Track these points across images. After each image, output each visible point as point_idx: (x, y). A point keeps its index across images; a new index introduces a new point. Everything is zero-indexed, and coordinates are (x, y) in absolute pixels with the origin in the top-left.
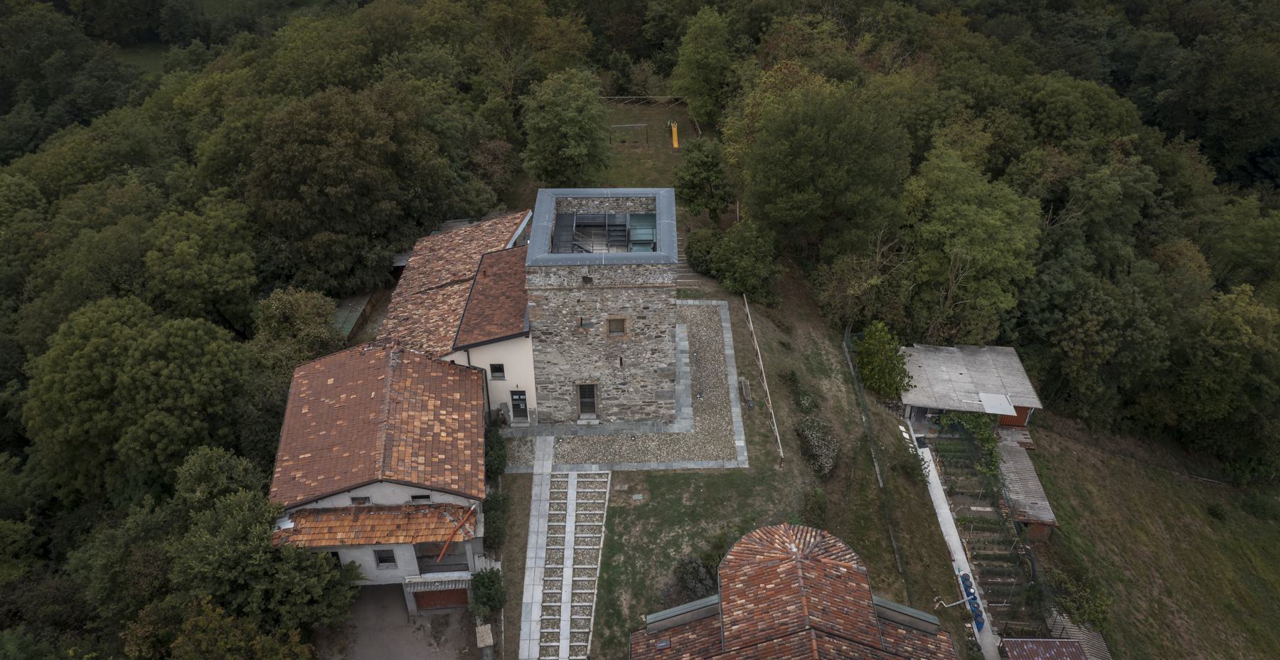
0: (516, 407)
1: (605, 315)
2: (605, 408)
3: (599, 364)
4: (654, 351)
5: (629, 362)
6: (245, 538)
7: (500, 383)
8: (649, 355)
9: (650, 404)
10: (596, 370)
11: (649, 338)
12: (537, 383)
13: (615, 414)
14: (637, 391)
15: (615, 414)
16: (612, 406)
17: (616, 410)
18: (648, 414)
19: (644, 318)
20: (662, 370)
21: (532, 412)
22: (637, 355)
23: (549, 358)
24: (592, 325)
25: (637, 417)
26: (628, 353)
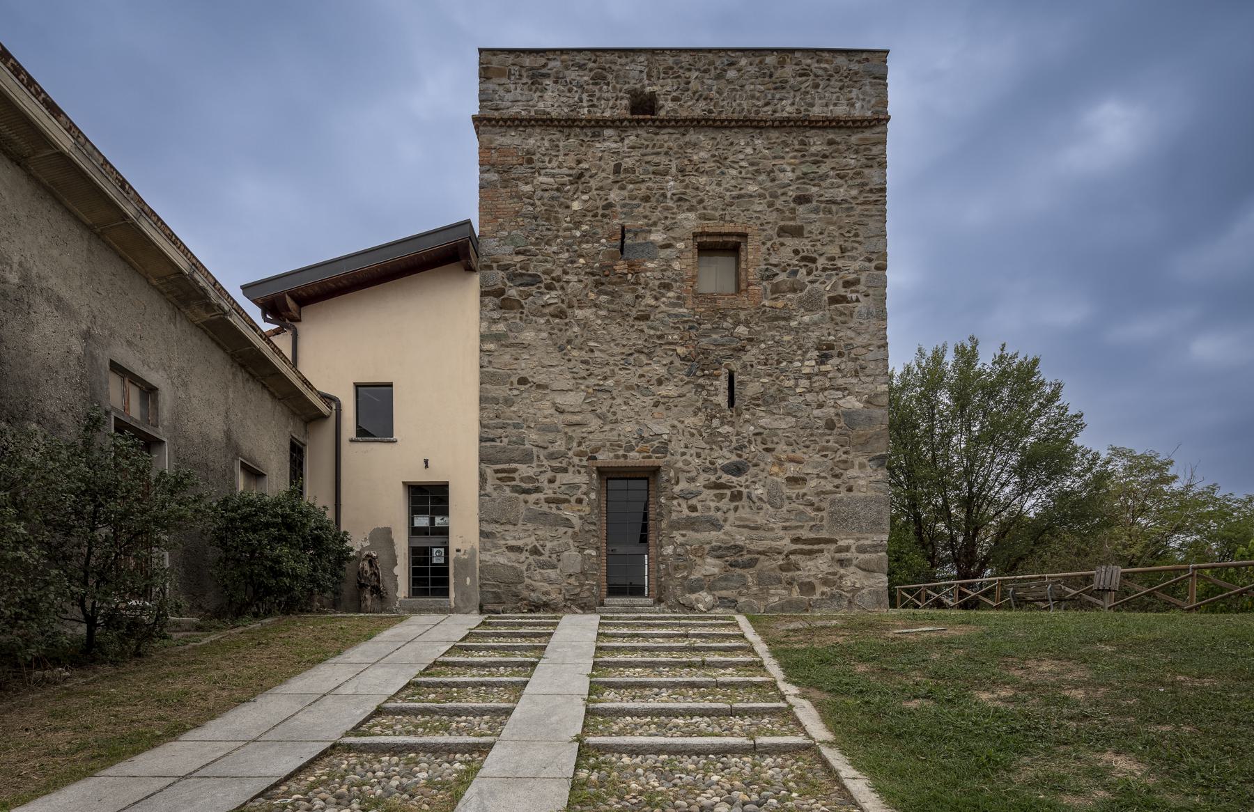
0: (419, 558)
1: (689, 221)
2: (684, 560)
3: (669, 390)
4: (825, 352)
5: (753, 388)
6: (18, 616)
7: (376, 451)
8: (809, 366)
9: (811, 547)
10: (655, 418)
11: (810, 304)
12: (484, 459)
13: (710, 585)
14: (774, 500)
15: (710, 585)
16: (699, 552)
17: (711, 567)
18: (808, 588)
19: (797, 232)
20: (849, 416)
21: (464, 565)
22: (777, 361)
23: (524, 367)
24: (651, 249)
25: (777, 595)
26: (752, 354)
